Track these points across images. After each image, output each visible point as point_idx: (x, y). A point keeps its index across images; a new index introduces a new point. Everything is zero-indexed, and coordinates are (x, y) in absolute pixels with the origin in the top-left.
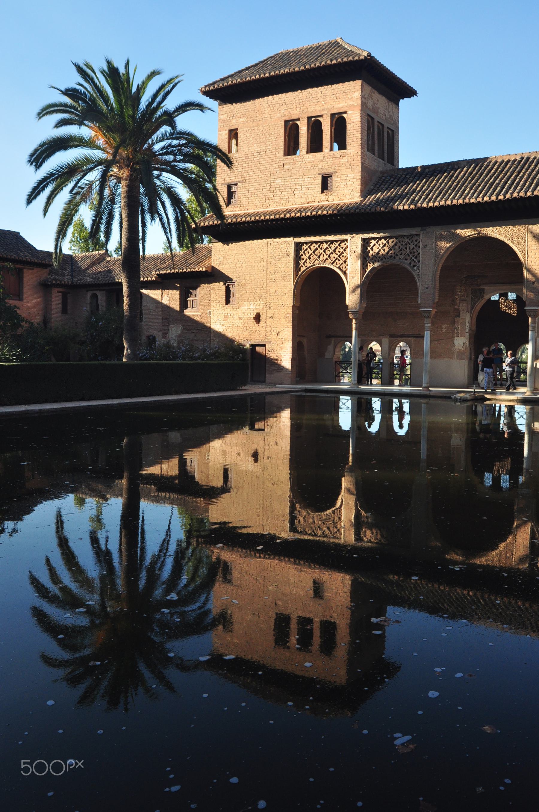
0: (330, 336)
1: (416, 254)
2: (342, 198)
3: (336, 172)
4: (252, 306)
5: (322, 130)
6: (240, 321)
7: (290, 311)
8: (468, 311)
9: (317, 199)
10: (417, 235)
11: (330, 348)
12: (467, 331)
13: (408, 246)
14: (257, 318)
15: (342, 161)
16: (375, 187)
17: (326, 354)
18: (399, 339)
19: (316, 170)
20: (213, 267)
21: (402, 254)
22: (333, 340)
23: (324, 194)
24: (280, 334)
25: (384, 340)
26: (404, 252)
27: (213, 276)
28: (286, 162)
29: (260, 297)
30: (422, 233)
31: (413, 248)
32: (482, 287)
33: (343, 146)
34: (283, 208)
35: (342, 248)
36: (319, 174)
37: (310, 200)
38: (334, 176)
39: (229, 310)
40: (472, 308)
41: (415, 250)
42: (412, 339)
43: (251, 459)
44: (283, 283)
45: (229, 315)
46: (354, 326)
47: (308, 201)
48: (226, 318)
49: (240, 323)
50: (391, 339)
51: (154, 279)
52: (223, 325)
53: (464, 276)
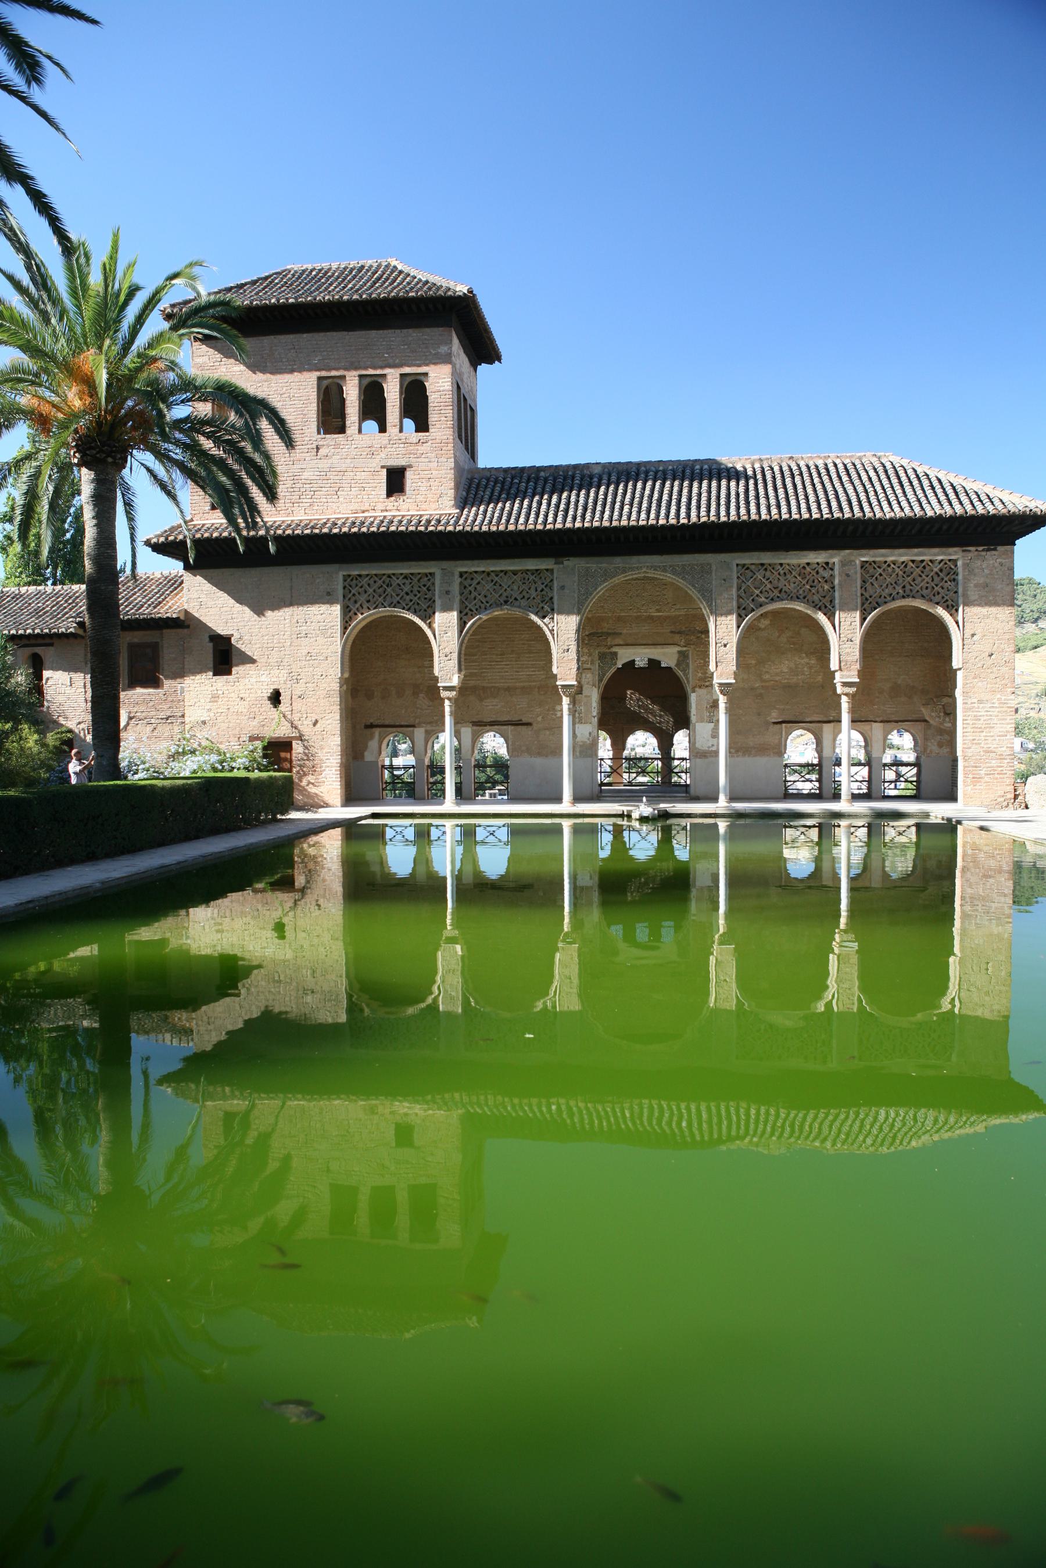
0: (372, 726)
1: (547, 599)
2: (423, 507)
3: (410, 466)
4: (263, 678)
5: (384, 400)
6: (242, 702)
7: (336, 686)
8: (594, 685)
9: (380, 506)
10: (547, 570)
11: (373, 744)
12: (595, 714)
13: (533, 588)
14: (275, 698)
15: (422, 449)
16: (468, 492)
17: (366, 754)
18: (488, 728)
19: (377, 460)
20: (186, 612)
22: (377, 732)
23: (392, 499)
24: (318, 725)
25: (463, 730)
26: (527, 596)
27: (188, 627)
28: (321, 443)
29: (279, 665)
30: (555, 567)
31: (542, 590)
32: (614, 649)
33: (422, 426)
34: (324, 518)
36: (382, 467)
37: (366, 507)
38: (409, 474)
39: (220, 684)
40: (600, 680)
42: (510, 728)
43: (270, 934)
44: (321, 640)
45: (220, 692)
46: (447, 709)
47: (363, 508)
48: (215, 698)
49: (242, 707)
50: (475, 728)
51: (72, 630)
52: (209, 710)
53: (587, 633)
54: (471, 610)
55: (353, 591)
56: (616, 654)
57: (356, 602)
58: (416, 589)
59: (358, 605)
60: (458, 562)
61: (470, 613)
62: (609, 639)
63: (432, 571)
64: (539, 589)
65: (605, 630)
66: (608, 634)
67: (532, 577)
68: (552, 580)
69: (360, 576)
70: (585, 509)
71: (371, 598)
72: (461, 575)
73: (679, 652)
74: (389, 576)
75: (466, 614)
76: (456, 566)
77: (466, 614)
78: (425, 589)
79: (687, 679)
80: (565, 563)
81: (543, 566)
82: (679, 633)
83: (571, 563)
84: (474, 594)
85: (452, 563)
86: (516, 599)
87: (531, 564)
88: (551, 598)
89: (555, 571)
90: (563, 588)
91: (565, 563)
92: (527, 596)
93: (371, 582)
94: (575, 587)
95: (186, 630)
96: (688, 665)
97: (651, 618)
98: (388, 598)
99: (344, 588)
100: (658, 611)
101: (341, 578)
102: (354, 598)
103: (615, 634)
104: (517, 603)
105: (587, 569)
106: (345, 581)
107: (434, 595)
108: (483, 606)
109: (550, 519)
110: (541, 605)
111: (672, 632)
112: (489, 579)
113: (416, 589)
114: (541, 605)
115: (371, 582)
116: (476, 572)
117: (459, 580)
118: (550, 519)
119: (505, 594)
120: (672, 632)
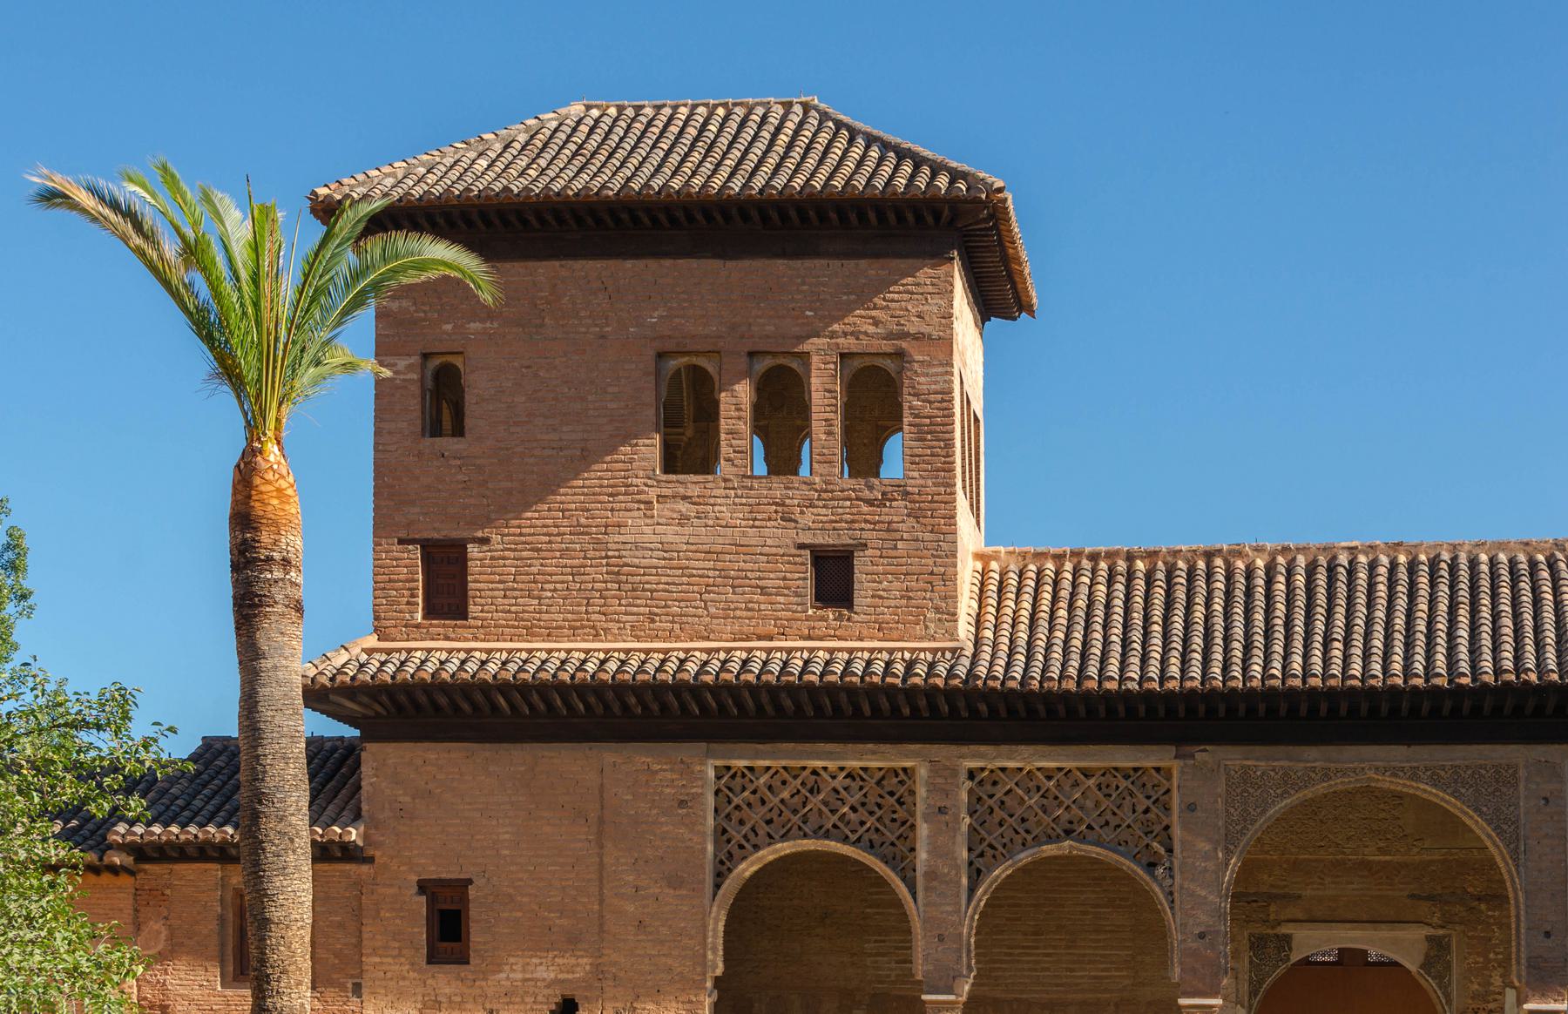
1: (1157, 828)
10: (1158, 770)
13: (1128, 802)
21: (1107, 823)
26: (1114, 821)
31: (1147, 811)
32: (1285, 930)
35: (892, 794)
41: (1150, 816)
54: (991, 846)
55: (736, 801)
56: (1287, 939)
57: (741, 822)
58: (872, 799)
59: (746, 829)
60: (964, 749)
61: (989, 852)
62: (1273, 908)
63: (908, 764)
64: (1140, 809)
65: (1264, 889)
66: (1272, 898)
67: (1124, 784)
68: (1168, 791)
69: (751, 769)
70: (1248, 647)
71: (774, 815)
72: (971, 775)
73: (1429, 939)
74: (815, 772)
75: (981, 855)
76: (963, 757)
77: (981, 855)
78: (892, 800)
79: (1447, 996)
80: (1198, 756)
81: (1148, 763)
82: (1430, 898)
83: (1207, 755)
84: (999, 814)
85: (953, 750)
86: (1090, 827)
87: (1123, 757)
88: (1167, 828)
89: (1175, 773)
90: (1191, 808)
91: (1198, 756)
92: (1114, 821)
93: (776, 783)
94: (1220, 804)
95: (365, 868)
96: (1448, 967)
97: (1365, 865)
98: (813, 818)
99: (717, 793)
100: (1382, 851)
101: (711, 773)
102: (736, 816)
103: (1284, 896)
104: (1091, 836)
105: (1246, 769)
106: (718, 778)
107: (913, 814)
108: (1018, 839)
109: (1174, 670)
110: (1146, 840)
111: (1412, 896)
112: (1031, 784)
113: (872, 799)
114: (1146, 840)
115: (776, 783)
116: (1003, 770)
117: (969, 784)
118: (1174, 670)
119: (1067, 816)
120: (1412, 896)
